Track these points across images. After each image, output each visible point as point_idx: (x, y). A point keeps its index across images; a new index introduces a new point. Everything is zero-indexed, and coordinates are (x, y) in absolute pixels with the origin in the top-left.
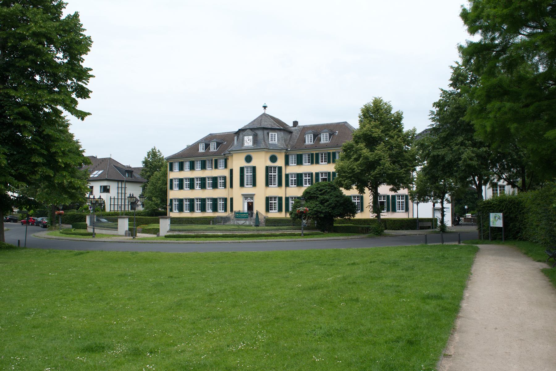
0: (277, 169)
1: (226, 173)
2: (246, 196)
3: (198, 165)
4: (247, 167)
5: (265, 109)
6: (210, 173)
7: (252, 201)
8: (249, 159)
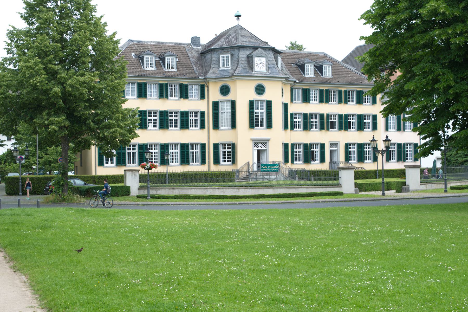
2: (256, 142)
3: (153, 91)
6: (174, 104)
7: (265, 148)
8: (260, 90)
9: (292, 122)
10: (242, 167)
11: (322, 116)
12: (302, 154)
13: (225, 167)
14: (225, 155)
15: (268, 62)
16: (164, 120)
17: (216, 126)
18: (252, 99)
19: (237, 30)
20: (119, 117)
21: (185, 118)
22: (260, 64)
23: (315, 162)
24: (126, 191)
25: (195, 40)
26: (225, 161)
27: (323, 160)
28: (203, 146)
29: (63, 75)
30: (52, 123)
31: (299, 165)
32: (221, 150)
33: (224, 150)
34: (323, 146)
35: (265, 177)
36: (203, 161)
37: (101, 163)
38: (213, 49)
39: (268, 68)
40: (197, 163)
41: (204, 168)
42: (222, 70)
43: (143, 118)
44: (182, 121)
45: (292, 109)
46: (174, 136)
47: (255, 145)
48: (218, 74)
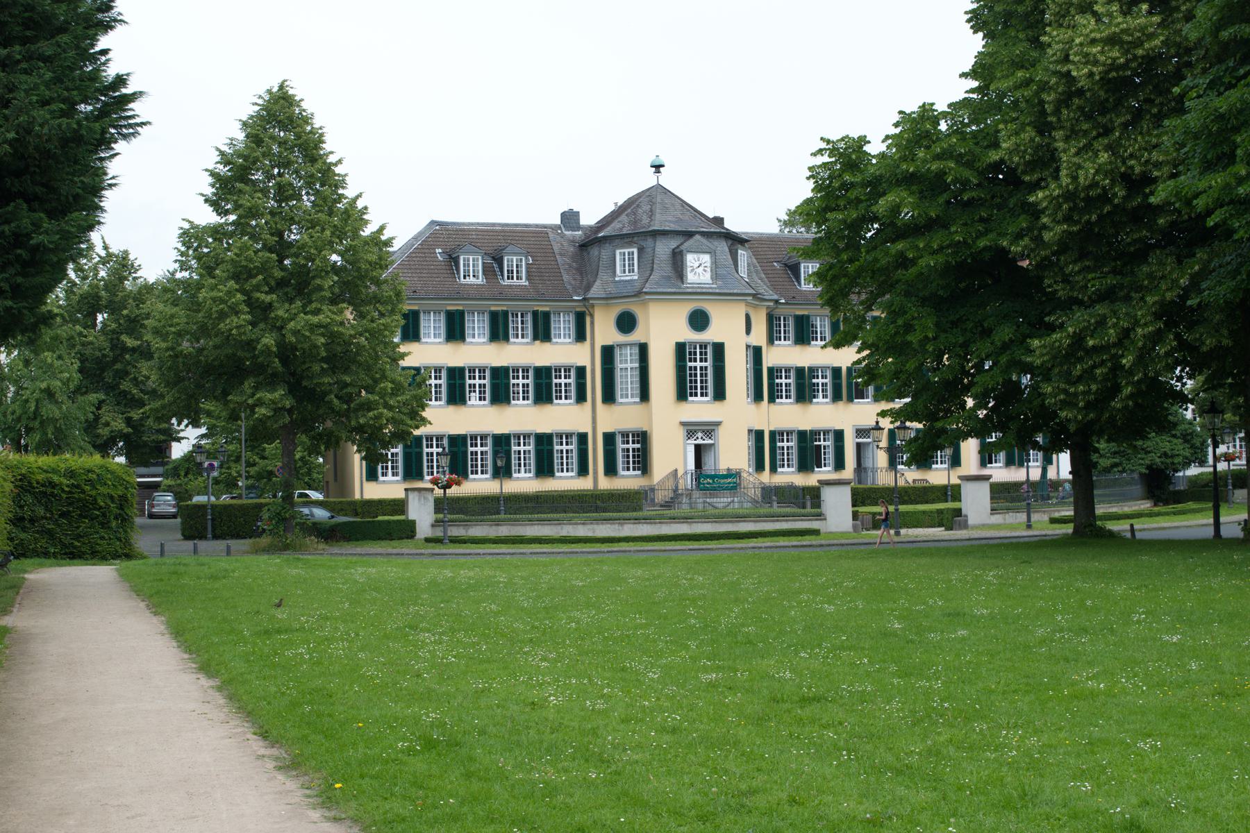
0: (709, 350)
2: (691, 429)
3: (477, 327)
6: (521, 352)
7: (710, 442)
8: (699, 320)
9: (771, 385)
10: (662, 481)
12: (795, 452)
13: (628, 480)
14: (628, 457)
15: (715, 265)
16: (500, 387)
17: (609, 396)
19: (656, 196)
20: (385, 389)
21: (544, 381)
22: (699, 268)
23: (824, 469)
24: (407, 530)
25: (570, 218)
26: (628, 469)
27: (840, 464)
29: (280, 313)
30: (260, 403)
31: (789, 476)
32: (620, 446)
33: (626, 446)
34: (839, 435)
36: (583, 470)
37: (372, 476)
38: (603, 237)
39: (716, 276)
40: (570, 474)
42: (620, 281)
43: (458, 382)
44: (538, 387)
45: (772, 358)
46: (522, 417)
47: (690, 434)
48: (611, 289)
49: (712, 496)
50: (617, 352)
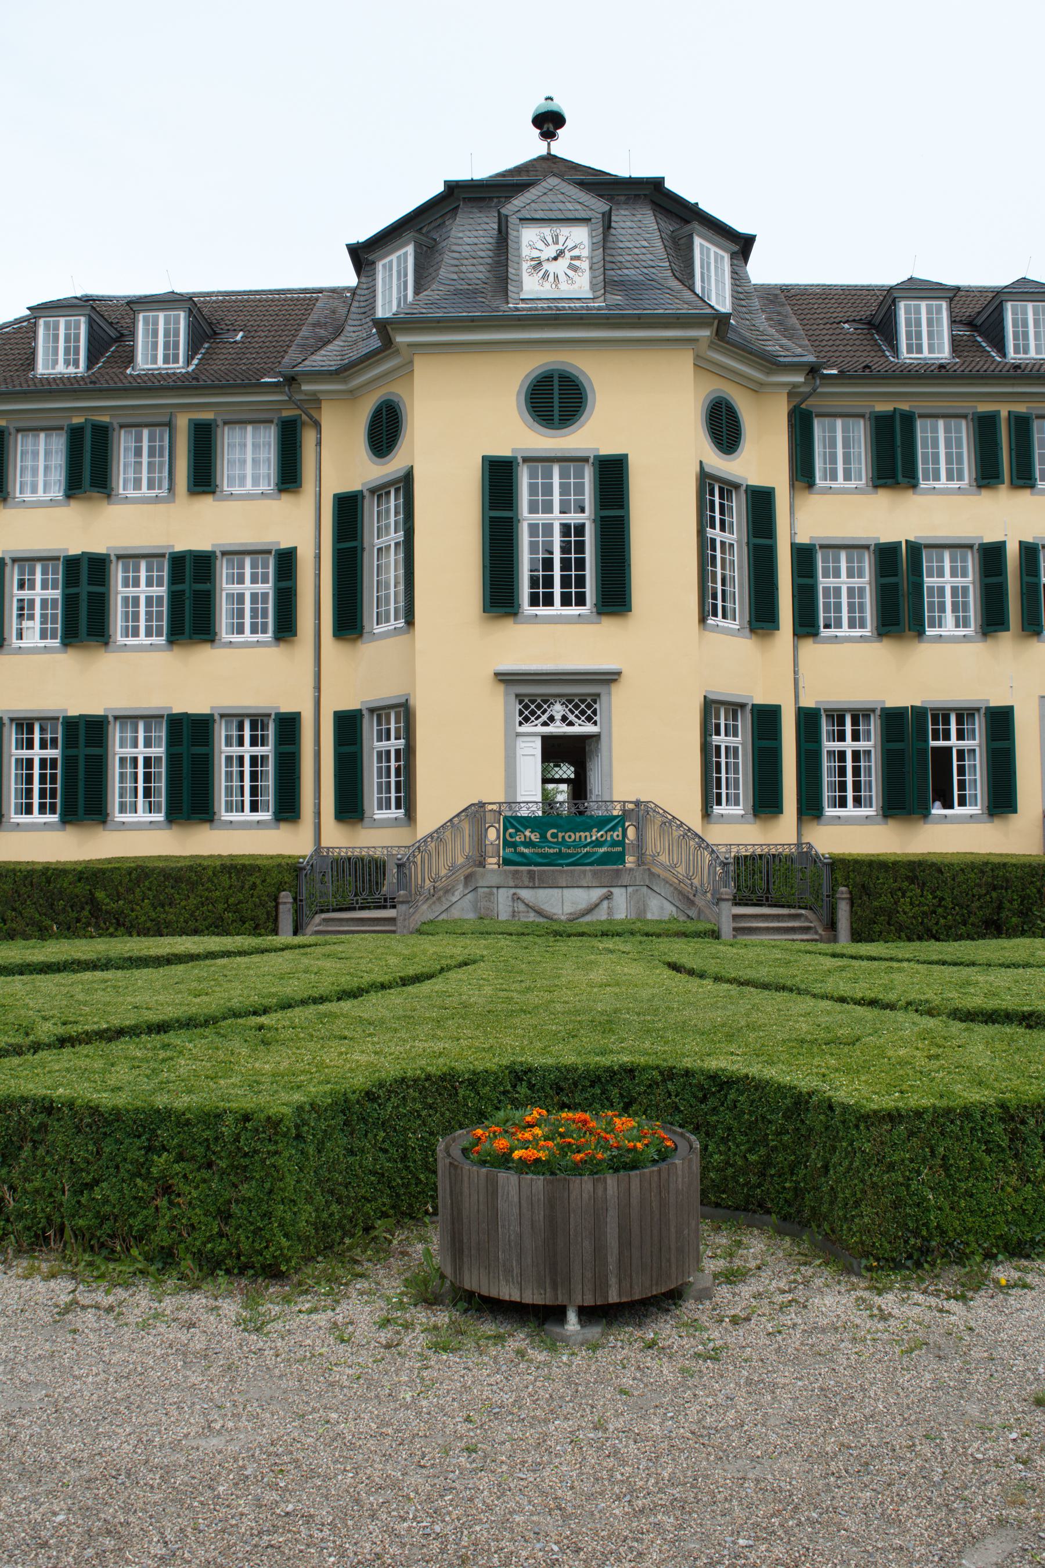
1: (298, 525)
2: (529, 692)
4: (541, 461)
5: (548, 135)
7: (589, 729)
8: (556, 399)
11: (992, 556)
12: (874, 765)
17: (349, 622)
18: (503, 451)
23: (958, 810)
28: (288, 726)
35: (524, 893)
41: (291, 843)
45: (802, 521)
47: (530, 707)
49: (536, 882)
50: (370, 509)
